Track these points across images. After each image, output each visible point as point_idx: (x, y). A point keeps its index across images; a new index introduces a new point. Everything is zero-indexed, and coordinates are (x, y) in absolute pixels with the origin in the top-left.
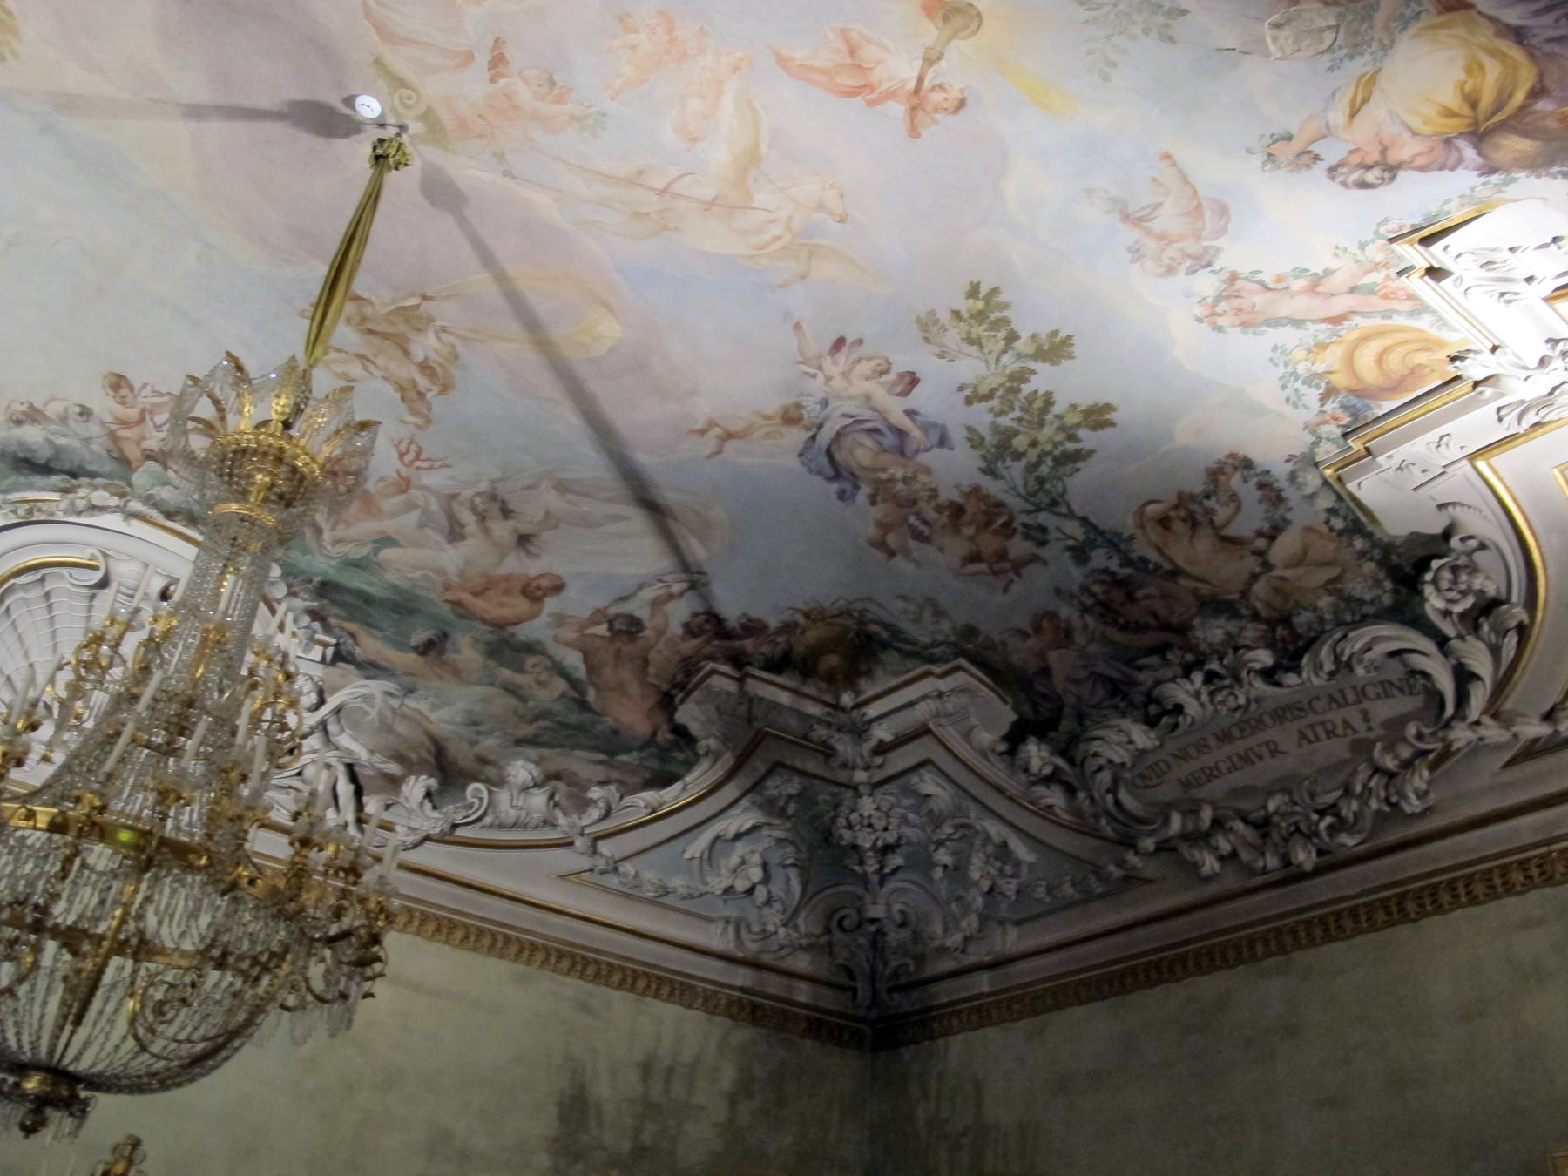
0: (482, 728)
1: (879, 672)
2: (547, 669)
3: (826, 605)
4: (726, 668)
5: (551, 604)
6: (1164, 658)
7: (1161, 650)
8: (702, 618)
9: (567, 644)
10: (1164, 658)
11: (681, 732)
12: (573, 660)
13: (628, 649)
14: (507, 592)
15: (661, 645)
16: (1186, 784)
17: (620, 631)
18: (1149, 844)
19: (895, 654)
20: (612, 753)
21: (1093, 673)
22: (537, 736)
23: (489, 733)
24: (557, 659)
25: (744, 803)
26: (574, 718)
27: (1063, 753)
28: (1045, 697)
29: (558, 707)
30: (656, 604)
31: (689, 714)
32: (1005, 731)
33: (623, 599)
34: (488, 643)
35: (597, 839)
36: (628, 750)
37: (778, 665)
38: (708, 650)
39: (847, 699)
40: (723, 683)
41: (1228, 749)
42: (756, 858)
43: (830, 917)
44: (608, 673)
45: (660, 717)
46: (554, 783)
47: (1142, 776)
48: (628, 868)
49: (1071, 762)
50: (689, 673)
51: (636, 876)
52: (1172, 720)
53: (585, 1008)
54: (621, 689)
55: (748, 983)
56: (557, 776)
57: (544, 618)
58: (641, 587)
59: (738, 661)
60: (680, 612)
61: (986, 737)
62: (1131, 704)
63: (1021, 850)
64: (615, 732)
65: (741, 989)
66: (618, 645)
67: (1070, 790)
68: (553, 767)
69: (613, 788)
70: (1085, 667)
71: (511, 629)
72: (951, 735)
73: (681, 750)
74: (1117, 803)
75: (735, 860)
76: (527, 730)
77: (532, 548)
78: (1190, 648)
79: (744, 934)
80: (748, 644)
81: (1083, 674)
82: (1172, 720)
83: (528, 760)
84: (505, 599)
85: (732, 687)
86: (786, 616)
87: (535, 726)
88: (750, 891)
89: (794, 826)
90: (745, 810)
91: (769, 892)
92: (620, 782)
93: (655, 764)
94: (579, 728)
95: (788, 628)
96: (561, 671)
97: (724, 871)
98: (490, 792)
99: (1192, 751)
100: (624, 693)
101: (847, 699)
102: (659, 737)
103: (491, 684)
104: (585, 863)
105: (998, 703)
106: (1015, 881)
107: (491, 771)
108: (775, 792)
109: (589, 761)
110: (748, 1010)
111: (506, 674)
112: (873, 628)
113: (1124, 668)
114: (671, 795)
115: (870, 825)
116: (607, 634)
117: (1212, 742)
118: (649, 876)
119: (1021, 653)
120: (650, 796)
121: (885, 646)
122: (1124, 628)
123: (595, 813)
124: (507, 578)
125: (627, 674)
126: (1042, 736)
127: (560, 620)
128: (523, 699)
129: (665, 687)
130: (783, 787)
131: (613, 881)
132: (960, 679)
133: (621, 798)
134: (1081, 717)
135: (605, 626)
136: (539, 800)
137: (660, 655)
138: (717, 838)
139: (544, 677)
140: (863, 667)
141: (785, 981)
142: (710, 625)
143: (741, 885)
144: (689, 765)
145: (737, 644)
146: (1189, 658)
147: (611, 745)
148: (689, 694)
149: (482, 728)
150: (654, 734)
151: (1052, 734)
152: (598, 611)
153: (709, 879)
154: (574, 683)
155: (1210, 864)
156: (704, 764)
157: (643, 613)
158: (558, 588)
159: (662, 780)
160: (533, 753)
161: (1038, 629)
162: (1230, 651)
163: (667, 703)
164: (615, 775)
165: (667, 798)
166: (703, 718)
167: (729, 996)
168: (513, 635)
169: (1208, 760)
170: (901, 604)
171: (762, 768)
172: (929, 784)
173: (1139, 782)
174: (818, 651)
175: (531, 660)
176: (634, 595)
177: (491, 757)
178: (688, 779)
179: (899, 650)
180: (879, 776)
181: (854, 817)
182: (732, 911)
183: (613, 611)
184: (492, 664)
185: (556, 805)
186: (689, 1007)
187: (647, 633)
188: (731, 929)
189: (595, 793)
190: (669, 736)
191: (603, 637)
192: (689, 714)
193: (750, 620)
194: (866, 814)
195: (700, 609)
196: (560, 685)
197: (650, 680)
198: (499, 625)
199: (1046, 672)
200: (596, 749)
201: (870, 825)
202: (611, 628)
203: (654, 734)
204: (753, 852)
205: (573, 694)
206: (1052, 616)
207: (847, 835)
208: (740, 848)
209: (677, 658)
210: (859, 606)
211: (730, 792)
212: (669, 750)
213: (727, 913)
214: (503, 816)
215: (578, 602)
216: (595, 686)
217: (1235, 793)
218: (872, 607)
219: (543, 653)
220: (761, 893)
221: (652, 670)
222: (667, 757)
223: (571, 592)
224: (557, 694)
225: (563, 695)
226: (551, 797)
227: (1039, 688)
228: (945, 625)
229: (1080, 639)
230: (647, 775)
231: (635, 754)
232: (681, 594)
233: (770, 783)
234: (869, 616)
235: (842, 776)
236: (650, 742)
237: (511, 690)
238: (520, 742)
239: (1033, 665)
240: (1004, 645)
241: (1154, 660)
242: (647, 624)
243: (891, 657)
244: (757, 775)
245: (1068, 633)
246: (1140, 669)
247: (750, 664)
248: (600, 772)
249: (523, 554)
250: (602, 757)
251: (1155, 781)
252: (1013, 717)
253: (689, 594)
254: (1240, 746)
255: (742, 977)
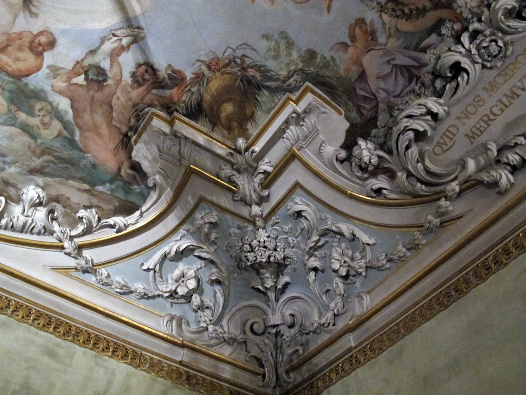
0: (8, 159)
1: (259, 114)
2: (50, 113)
3: (220, 55)
4: (162, 114)
5: (49, 58)
6: (440, 35)
7: (436, 28)
8: (144, 67)
9: (60, 93)
10: (440, 35)
11: (136, 167)
12: (64, 104)
13: (99, 96)
14: (20, 49)
15: (119, 93)
16: (471, 137)
17: (92, 80)
18: (455, 186)
19: (266, 92)
20: (93, 184)
21: (395, 66)
22: (45, 167)
23: (10, 164)
24: (55, 104)
25: (182, 231)
26: (68, 153)
27: (381, 146)
28: (365, 98)
29: (57, 144)
30: (114, 55)
31: (143, 153)
32: (342, 140)
33: (93, 52)
34: (11, 91)
35: (80, 248)
36: (103, 183)
37: (195, 112)
38: (148, 98)
39: (241, 143)
40: (159, 124)
41: (498, 95)
42: (191, 273)
43: (244, 324)
44: (87, 117)
45: (122, 155)
46: (54, 204)
47: (439, 144)
48: (104, 271)
49: (390, 152)
50: (138, 118)
51: (109, 276)
52: (454, 84)
53: (51, 354)
54: (96, 130)
55: (185, 359)
56: (57, 200)
57: (44, 70)
58: (103, 40)
59: (169, 108)
60: (128, 61)
61: (331, 150)
62: (423, 85)
63: (364, 238)
64: (94, 166)
65: (180, 363)
66: (91, 93)
67: (391, 175)
68: (54, 193)
69: (94, 210)
70: (388, 62)
71: (25, 80)
72: (308, 155)
73: (138, 184)
74: (426, 169)
75: (177, 273)
76: (37, 162)
77: (34, 9)
78: (459, 18)
79: (184, 326)
80: (173, 93)
81: (387, 69)
82: (454, 84)
83: (37, 185)
84: (20, 55)
85: (166, 129)
86: (195, 68)
87: (41, 159)
88: (188, 297)
89: (216, 250)
90: (183, 236)
91: (202, 301)
92: (97, 207)
93: (120, 194)
94: (72, 163)
95: (199, 77)
96: (58, 116)
97: (170, 281)
98: (6, 201)
99: (471, 109)
100: (99, 134)
101: (241, 143)
102: (123, 173)
103: (12, 125)
104: (71, 262)
105: (335, 115)
106: (363, 261)
107: (12, 191)
108: (202, 222)
109: (79, 189)
110: (184, 377)
111: (22, 116)
112: (251, 72)
113: (414, 54)
114: (133, 221)
115: (265, 247)
116: (85, 83)
117: (484, 95)
118: (118, 279)
119: (343, 64)
120: (119, 220)
121: (259, 87)
122: (409, 17)
123: (81, 228)
124: (20, 36)
125: (100, 119)
126: (366, 137)
127: (55, 71)
128: (34, 137)
129: (124, 129)
130: (205, 216)
131: (92, 279)
132: (309, 98)
133: (99, 220)
134: (390, 108)
135: (83, 76)
136: (41, 214)
137: (120, 100)
138: (165, 256)
139: (46, 119)
140: (248, 113)
141: (213, 362)
142: (146, 73)
143: (182, 291)
144: (144, 198)
145: (167, 93)
146: (457, 27)
147: (91, 177)
148: (139, 136)
149: (8, 159)
150: (119, 169)
151: (374, 131)
152: (78, 62)
153: (160, 287)
154: (65, 124)
155: (505, 177)
156: (154, 196)
157: (105, 64)
158: (52, 44)
159: (127, 209)
160: (40, 180)
161: (353, 38)
162: (485, 9)
163: (126, 144)
164: (95, 201)
165: (129, 222)
166: (150, 157)
167: (170, 365)
168: (26, 85)
169: (483, 110)
170: (265, 43)
171: (192, 202)
172: (299, 203)
173: (438, 150)
174: (220, 99)
175: (38, 106)
176: (99, 48)
177: (12, 181)
178: (144, 209)
179: (268, 88)
180: (267, 208)
181: (255, 243)
182: (176, 311)
183: (86, 63)
184: (13, 108)
185: (53, 219)
186: (138, 366)
187: (109, 82)
188: (174, 322)
189: (82, 213)
190: (130, 171)
191: (81, 86)
192: (143, 153)
193: (173, 72)
194: (262, 240)
195: (141, 61)
196: (57, 126)
197: (114, 123)
198: (18, 76)
199: (362, 76)
200: (82, 180)
201: (265, 247)
202: (87, 79)
203: (119, 169)
204: (190, 269)
205: (65, 133)
206: (361, 22)
207: (251, 256)
208: (181, 267)
209: (130, 103)
210: (239, 53)
211: (171, 221)
212: (130, 184)
213: (174, 314)
214: (15, 220)
215: (65, 55)
216: (80, 128)
217: (509, 126)
218: (249, 52)
219: (45, 100)
220: (196, 300)
221: (114, 114)
222: (128, 189)
223: (60, 48)
224: (56, 133)
225: (59, 135)
226: (51, 211)
227: (362, 93)
228: (295, 55)
229: (382, 39)
230: (117, 204)
231: (108, 185)
232: (128, 47)
233: (198, 215)
234: (248, 61)
235: (244, 211)
236: (116, 176)
237: (26, 129)
238: (33, 171)
239: (355, 70)
240: (333, 59)
241: (433, 38)
242: (109, 75)
243: (264, 97)
244: (190, 207)
245: (373, 34)
246: (424, 50)
247: (178, 111)
248: (84, 198)
249: (28, 14)
250: (86, 187)
251: (450, 144)
252: (346, 125)
253: (133, 46)
254: (505, 89)
255: (181, 355)
